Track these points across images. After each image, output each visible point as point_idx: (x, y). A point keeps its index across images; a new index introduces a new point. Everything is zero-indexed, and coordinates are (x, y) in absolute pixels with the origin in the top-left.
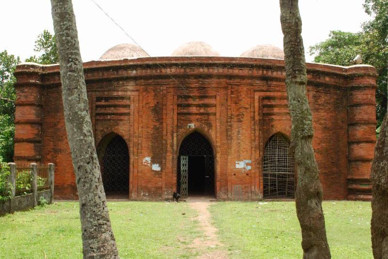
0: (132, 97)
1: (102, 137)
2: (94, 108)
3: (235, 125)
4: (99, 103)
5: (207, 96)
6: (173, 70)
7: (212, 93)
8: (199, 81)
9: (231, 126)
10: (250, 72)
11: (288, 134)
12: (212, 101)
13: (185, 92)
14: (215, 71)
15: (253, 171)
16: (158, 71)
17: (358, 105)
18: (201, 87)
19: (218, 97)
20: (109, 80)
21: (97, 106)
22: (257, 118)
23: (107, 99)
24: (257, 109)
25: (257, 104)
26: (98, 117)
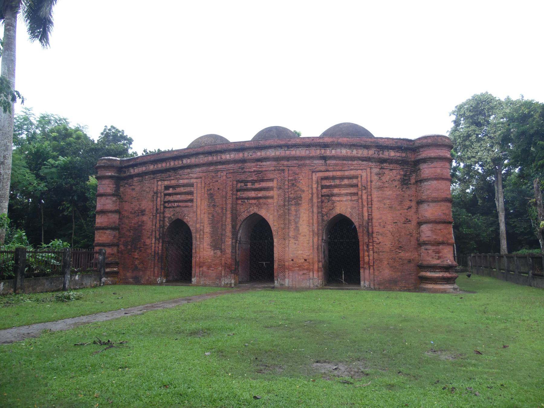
0: (195, 184)
2: (163, 197)
3: (293, 208)
4: (167, 192)
7: (271, 176)
8: (257, 165)
9: (289, 210)
10: (307, 152)
11: (348, 216)
12: (270, 184)
13: (243, 177)
14: (271, 153)
15: (311, 256)
16: (219, 157)
17: (427, 180)
19: (275, 182)
20: (175, 169)
21: (165, 195)
22: (315, 200)
23: (174, 187)
24: (315, 191)
25: (315, 186)
26: (166, 205)
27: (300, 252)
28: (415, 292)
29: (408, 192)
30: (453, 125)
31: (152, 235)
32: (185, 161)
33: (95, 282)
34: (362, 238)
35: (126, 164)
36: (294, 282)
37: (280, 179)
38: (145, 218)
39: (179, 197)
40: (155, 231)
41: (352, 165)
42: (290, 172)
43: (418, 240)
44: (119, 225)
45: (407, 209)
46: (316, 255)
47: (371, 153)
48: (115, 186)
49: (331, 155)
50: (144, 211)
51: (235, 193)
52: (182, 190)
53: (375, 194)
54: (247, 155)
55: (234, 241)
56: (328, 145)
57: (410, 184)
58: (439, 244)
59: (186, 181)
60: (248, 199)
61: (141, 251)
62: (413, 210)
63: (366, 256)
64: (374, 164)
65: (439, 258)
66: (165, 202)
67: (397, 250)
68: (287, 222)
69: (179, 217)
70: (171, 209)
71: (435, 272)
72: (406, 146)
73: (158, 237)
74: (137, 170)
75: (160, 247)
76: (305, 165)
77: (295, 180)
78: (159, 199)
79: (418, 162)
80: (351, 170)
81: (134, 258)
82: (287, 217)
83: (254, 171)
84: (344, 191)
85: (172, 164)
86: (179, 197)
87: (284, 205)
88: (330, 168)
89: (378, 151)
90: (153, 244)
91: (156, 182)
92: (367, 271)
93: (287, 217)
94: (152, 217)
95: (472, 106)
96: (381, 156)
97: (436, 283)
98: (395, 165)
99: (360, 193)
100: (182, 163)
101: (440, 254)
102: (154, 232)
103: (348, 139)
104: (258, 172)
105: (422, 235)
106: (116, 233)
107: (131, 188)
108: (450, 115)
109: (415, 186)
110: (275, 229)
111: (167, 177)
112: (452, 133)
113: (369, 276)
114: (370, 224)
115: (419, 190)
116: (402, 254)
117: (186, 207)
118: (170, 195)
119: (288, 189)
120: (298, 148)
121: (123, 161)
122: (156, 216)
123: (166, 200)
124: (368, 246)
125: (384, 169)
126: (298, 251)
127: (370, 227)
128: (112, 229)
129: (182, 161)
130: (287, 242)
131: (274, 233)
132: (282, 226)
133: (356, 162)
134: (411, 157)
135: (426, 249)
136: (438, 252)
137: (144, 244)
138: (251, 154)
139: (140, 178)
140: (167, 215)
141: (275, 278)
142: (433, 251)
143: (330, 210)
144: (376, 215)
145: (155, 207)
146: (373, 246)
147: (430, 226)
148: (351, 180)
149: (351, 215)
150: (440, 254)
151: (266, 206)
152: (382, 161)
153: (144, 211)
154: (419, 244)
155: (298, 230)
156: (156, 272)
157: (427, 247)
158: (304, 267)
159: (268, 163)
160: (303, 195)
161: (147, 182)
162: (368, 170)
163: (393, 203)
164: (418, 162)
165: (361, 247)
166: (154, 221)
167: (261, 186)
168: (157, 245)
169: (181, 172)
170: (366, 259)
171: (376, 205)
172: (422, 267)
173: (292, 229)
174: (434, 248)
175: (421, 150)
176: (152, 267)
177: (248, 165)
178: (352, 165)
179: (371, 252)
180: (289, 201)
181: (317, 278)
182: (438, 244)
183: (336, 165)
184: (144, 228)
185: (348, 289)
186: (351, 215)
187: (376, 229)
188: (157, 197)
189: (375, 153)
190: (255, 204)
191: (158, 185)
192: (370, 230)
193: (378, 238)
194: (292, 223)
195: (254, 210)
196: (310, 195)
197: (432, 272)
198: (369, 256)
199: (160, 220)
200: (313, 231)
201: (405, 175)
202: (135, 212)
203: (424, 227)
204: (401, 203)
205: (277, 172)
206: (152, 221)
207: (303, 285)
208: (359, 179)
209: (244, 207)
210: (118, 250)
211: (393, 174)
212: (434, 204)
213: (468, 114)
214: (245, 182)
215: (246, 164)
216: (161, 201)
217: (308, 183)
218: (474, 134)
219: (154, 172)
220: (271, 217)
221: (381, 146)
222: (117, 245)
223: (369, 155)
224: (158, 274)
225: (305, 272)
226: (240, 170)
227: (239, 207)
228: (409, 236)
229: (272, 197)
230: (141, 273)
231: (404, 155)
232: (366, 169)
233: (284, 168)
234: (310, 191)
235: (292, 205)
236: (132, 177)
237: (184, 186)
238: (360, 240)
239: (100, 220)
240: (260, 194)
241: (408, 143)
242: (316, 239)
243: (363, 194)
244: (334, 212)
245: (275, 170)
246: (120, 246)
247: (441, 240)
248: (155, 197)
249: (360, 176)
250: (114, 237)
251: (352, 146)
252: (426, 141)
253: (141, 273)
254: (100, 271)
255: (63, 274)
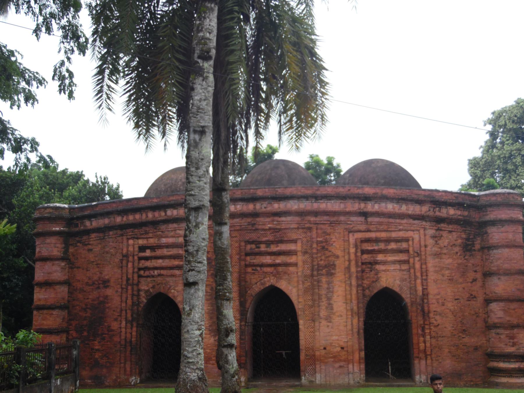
1: (146, 299)
2: (137, 261)
3: (324, 279)
4: (142, 254)
5: (284, 241)
6: (238, 206)
7: (294, 236)
8: (273, 221)
9: (319, 281)
10: (342, 206)
11: (397, 289)
12: (291, 247)
13: (253, 236)
14: (293, 205)
17: (496, 247)
18: (277, 229)
19: (299, 244)
20: (155, 223)
21: (140, 259)
22: (353, 269)
23: (153, 248)
24: (353, 257)
25: (352, 250)
26: (142, 272)
27: (335, 338)
28: (484, 387)
29: (472, 261)
30: (487, 137)
31: (120, 316)
32: (169, 212)
33: (71, 388)
34: (415, 318)
35: (80, 214)
36: (328, 378)
37: (305, 240)
38: (109, 292)
39: (160, 262)
40: (126, 311)
41: (400, 224)
42: (320, 231)
43: (486, 322)
44: (69, 301)
45: (472, 282)
46: (356, 341)
47: (424, 209)
48: (63, 245)
49: (374, 210)
50: (108, 281)
51: (243, 257)
52: (165, 252)
53: (431, 263)
54: (259, 206)
55: (243, 323)
56: (369, 197)
57: (475, 250)
58: (513, 327)
59: (171, 240)
60: (262, 265)
61: (103, 339)
62: (479, 283)
63: (420, 342)
64: (428, 224)
65: (514, 344)
66: (140, 269)
67: (460, 334)
68: (316, 297)
69: (162, 291)
70: (149, 279)
71: (509, 362)
72: (469, 203)
73: (129, 318)
74: (95, 223)
75: (134, 334)
76: (339, 223)
77: (326, 241)
78: (130, 265)
79: (484, 224)
80: (400, 230)
81: (92, 349)
82: (317, 290)
83: (270, 229)
84: (391, 258)
85: (150, 215)
86: (160, 262)
87: (312, 275)
88: (372, 227)
89: (434, 208)
90: (123, 328)
91: (125, 240)
92: (423, 362)
93: (317, 290)
94: (120, 290)
95: (516, 116)
96: (438, 213)
97: (511, 376)
98: (455, 226)
99: (411, 260)
100: (166, 215)
101: (515, 340)
102: (124, 312)
103: (395, 191)
104: (275, 230)
105: (492, 315)
106: (65, 313)
107: (86, 248)
108: (485, 125)
109: (480, 254)
110: (300, 307)
111: (142, 234)
112: (488, 151)
113: (426, 369)
114: (426, 301)
115: (487, 259)
116: (466, 340)
117: (173, 276)
118: (147, 259)
119: (317, 253)
120: (330, 200)
121: (74, 209)
122: (127, 289)
123: (141, 265)
124: (423, 329)
125: (441, 230)
126: (332, 336)
127: (426, 305)
128: (61, 308)
129: (165, 212)
130: (317, 324)
131: (299, 313)
132: (310, 303)
133: (405, 221)
134: (475, 216)
135: (498, 334)
136: (512, 338)
137: (109, 329)
138: (265, 205)
139: (101, 235)
140: (144, 287)
141: (302, 374)
142: (507, 336)
143: (373, 282)
144: (433, 289)
145: (125, 275)
146: (430, 329)
147: (502, 304)
148: (400, 244)
149: (401, 289)
150: (515, 340)
151: (287, 277)
152: (439, 220)
153: (108, 281)
154: (486, 327)
155: (332, 309)
156: (128, 369)
157: (498, 331)
158: (340, 358)
159: (289, 218)
160: (337, 263)
161: (111, 240)
162: (422, 231)
163: (453, 274)
164: (484, 224)
165: (414, 331)
166: (124, 295)
167: (279, 248)
168: (129, 330)
169: (163, 227)
170: (422, 346)
171: (432, 276)
172: (492, 356)
173: (324, 308)
174: (508, 332)
175: (489, 209)
176: (122, 361)
177: (261, 220)
178: (400, 224)
179: (428, 337)
180: (318, 270)
181: (356, 372)
182: (512, 327)
183: (380, 224)
184: (107, 305)
185: (399, 386)
186: (401, 289)
187: (434, 307)
188: (128, 261)
189: (429, 210)
190: (272, 273)
191: (128, 245)
192: (426, 309)
193: (436, 319)
194: (324, 300)
195: (270, 281)
196: (347, 263)
197: (506, 362)
198: (425, 342)
199: (133, 295)
200: (352, 310)
201: (467, 239)
202: (94, 283)
203: (494, 306)
204: (464, 274)
205: (301, 230)
206: (121, 297)
207: (340, 381)
208: (411, 243)
209: (256, 276)
210: (67, 338)
211: (452, 237)
212: (506, 278)
213: (510, 125)
214: (257, 243)
215: (258, 219)
216: (134, 267)
217: (343, 247)
218: (519, 154)
219: (122, 227)
220: (295, 290)
221: (438, 201)
222: (66, 331)
223: (423, 213)
224: (131, 371)
225: (342, 364)
226: (250, 227)
227: (248, 277)
228: (475, 317)
229: (296, 265)
230: (104, 370)
231: (466, 213)
232: (418, 231)
233: (311, 226)
234: (347, 257)
235: (322, 275)
236: (88, 232)
237: (168, 246)
238: (414, 321)
239: (40, 296)
240: (279, 260)
241: (471, 199)
242: (355, 321)
243: (416, 261)
244: (378, 285)
245: (298, 228)
246: (71, 332)
247: (515, 321)
248: (124, 262)
249: (411, 239)
250: (64, 319)
251: (400, 200)
252: (493, 199)
253: (104, 370)
254: (74, 372)
255: (47, 377)
